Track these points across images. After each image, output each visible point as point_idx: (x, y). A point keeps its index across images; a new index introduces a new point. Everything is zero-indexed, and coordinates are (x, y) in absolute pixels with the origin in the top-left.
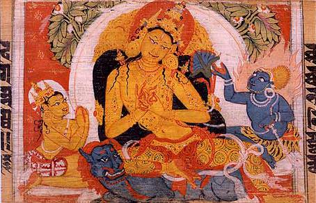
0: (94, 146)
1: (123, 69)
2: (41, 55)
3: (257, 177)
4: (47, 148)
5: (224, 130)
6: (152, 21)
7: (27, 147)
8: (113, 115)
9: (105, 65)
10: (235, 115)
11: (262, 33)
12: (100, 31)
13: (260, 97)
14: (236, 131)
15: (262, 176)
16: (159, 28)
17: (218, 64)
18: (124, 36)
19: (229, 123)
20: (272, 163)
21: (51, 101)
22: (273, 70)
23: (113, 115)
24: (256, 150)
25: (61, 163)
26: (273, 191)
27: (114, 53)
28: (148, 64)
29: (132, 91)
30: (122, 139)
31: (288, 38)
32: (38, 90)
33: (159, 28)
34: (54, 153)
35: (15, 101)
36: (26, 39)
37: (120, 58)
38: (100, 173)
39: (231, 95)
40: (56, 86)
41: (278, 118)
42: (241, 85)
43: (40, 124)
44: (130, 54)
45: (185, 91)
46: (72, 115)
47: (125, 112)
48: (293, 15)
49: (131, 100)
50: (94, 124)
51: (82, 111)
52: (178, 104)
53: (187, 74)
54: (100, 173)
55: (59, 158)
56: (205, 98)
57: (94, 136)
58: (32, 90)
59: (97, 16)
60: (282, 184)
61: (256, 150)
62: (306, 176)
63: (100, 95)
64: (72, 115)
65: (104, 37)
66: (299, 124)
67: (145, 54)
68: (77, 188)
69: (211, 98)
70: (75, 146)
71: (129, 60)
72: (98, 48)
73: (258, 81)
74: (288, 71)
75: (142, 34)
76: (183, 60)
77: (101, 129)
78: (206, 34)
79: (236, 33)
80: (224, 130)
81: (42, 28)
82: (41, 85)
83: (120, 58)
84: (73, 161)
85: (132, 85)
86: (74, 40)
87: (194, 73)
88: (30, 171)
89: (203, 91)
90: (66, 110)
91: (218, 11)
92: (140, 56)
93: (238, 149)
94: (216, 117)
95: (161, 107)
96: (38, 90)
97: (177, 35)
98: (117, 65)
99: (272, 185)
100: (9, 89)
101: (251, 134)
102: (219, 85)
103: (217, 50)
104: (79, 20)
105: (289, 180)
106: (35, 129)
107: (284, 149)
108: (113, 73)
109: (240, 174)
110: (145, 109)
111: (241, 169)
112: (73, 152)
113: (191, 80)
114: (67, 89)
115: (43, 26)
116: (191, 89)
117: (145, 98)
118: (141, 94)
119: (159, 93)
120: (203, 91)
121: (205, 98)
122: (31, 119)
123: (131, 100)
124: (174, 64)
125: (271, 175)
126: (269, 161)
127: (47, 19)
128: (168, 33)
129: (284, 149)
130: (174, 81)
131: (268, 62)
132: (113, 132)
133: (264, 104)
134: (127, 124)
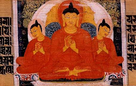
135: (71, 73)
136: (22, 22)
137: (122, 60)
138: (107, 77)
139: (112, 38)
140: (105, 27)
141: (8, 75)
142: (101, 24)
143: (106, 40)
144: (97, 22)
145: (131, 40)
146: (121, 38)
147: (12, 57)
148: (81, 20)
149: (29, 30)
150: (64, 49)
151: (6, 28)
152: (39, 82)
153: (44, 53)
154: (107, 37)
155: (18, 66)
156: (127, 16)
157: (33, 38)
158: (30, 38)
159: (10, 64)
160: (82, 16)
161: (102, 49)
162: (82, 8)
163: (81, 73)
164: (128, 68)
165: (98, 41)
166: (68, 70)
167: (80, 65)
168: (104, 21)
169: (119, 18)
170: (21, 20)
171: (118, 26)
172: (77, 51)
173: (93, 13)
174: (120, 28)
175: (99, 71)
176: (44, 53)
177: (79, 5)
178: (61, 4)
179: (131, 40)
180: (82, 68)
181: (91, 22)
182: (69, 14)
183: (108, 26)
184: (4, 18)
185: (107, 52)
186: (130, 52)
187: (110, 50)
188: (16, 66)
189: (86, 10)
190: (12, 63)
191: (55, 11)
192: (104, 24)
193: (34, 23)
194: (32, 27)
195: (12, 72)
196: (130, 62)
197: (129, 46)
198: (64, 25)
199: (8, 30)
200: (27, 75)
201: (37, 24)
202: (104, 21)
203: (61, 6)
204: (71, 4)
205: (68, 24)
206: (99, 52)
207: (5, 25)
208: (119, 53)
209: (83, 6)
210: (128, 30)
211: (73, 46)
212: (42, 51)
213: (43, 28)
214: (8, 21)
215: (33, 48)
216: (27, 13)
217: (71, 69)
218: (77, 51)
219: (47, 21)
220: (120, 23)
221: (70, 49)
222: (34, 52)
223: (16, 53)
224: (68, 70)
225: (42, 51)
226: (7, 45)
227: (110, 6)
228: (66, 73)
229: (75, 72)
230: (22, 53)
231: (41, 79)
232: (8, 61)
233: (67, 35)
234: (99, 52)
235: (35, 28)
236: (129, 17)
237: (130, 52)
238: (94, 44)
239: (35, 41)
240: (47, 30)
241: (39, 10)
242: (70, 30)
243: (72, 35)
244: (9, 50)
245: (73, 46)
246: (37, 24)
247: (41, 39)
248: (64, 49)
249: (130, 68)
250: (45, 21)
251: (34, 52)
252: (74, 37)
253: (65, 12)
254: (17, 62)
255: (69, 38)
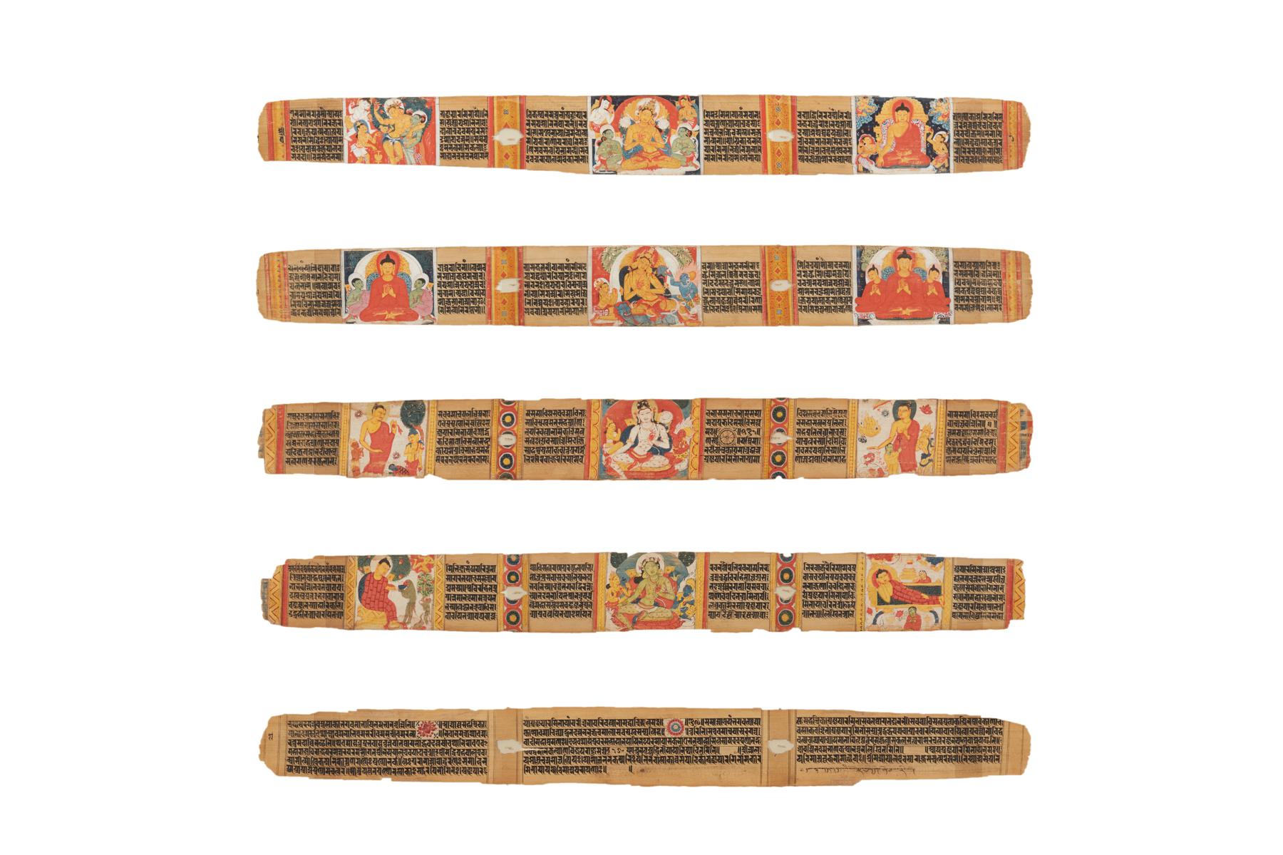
0: (620, 303)
1: (631, 273)
2: (599, 268)
3: (684, 315)
4: (601, 305)
5: (670, 296)
6: (642, 255)
7: (593, 304)
8: (627, 291)
9: (624, 272)
10: (675, 290)
11: (686, 259)
12: (621, 259)
13: (685, 284)
14: (675, 297)
15: (686, 314)
16: (645, 257)
17: (668, 271)
18: (631, 260)
19: (672, 293)
20: (689, 309)
21: (603, 286)
22: (690, 273)
23: (627, 291)
24: (684, 304)
25: (607, 310)
26: (690, 320)
27: (627, 267)
28: (640, 271)
29: (634, 282)
30: (630, 301)
31: (695, 261)
32: (597, 282)
33: (645, 257)
34: (604, 307)
35: (588, 286)
36: (593, 262)
37: (629, 269)
38: (622, 314)
39: (673, 283)
40: (605, 280)
41: (692, 292)
42: (677, 279)
43: (598, 295)
44: (634, 267)
45: (655, 281)
46: (611, 292)
47: (632, 290)
48: (697, 252)
49: (634, 285)
50: (620, 295)
51: (615, 290)
52: (652, 287)
53: (656, 275)
54: (622, 314)
55: (606, 308)
56: (663, 284)
57: (620, 300)
58: (595, 282)
59: (620, 253)
60: (694, 317)
61: (684, 304)
62: (703, 314)
63: (622, 283)
64: (611, 292)
65: (623, 260)
66: (700, 294)
67: (639, 267)
68: (613, 320)
69: (665, 284)
70: (612, 304)
71: (633, 270)
72: (620, 266)
73: (684, 277)
74: (695, 273)
75: (638, 259)
76: (654, 269)
77: (623, 297)
78: (663, 259)
79: (675, 258)
80: (670, 296)
81: (599, 258)
82: (599, 280)
83: (629, 269)
84: (611, 310)
85: (634, 279)
86: (612, 261)
87: (659, 274)
88: (595, 314)
89: (662, 281)
90: (608, 290)
91: (668, 250)
92: (637, 268)
93: (676, 304)
94: (667, 291)
95: (646, 288)
96: (597, 282)
97: (652, 259)
98: (628, 272)
99: (690, 318)
100: (586, 282)
101: (681, 298)
102: (668, 279)
103: (667, 266)
104: (613, 254)
105: (696, 316)
106: (597, 297)
107: (694, 303)
108: (627, 275)
109: (677, 313)
110: (639, 289)
111: (677, 312)
112: (611, 306)
113: (658, 277)
114: (609, 281)
115: (599, 257)
116: (657, 281)
117: (639, 285)
118: (638, 283)
119: (645, 282)
120: (662, 281)
121: (663, 284)
122: (595, 294)
123: (634, 285)
124: (651, 271)
125: (689, 314)
126: (687, 309)
127: (600, 255)
128: (648, 259)
129: (694, 303)
130: (651, 278)
131: (687, 270)
132: (627, 298)
133: (686, 286)
134: (632, 295)
135: (904, 312)
136: (861, 265)
137: (950, 301)
138: (936, 316)
139: (941, 281)
140: (935, 271)
141: (847, 313)
142: (931, 269)
143: (936, 283)
144: (928, 266)
145: (958, 283)
146: (948, 281)
147: (851, 298)
148: (913, 265)
149: (866, 273)
150: (898, 291)
151: (846, 271)
152: (875, 319)
153: (880, 294)
154: (937, 280)
155: (856, 305)
156: (955, 262)
157: (871, 281)
158: (867, 281)
159: (849, 304)
160: (914, 261)
161: (932, 291)
162: (914, 254)
163: (913, 313)
164: (955, 308)
165: (928, 284)
166: (901, 309)
167: (912, 306)
168: (934, 266)
169: (948, 264)
170: (860, 264)
171: (946, 271)
172: (909, 292)
173: (924, 259)
174: (948, 273)
175: (929, 310)
176: (880, 294)
177: (912, 251)
178: (896, 251)
179: (958, 283)
180: (914, 307)
181: (923, 267)
182: (902, 260)
183: (938, 271)
184: (845, 262)
185: (936, 293)
186: (956, 294)
187: (938, 292)
188: (854, 305)
189: (918, 256)
190: (851, 303)
191: (890, 257)
192: (933, 268)
193: (871, 267)
194: (870, 270)
195: (851, 311)
196: (956, 303)
197: (956, 288)
198: (898, 269)
199: (848, 273)
200: (864, 314)
201: (873, 268)
202: (934, 266)
203: (896, 252)
204: (905, 250)
205: (902, 268)
206: (929, 294)
207: (845, 269)
208: (947, 295)
209: (916, 252)
210: (955, 274)
211: (906, 289)
212: (878, 292)
213: (879, 271)
214: (848, 264)
215: (870, 290)
216: (865, 258)
217: (904, 308)
218: (909, 292)
219: (883, 266)
220: (948, 268)
221: (903, 291)
222: (871, 293)
223: (855, 294)
224: (901, 309)
225: (878, 292)
226: (847, 287)
227: (939, 253)
228: (899, 312)
229: (908, 312)
230: (860, 294)
231: (877, 318)
232: (848, 301)
233: (901, 278)
234: (929, 294)
235: (872, 271)
236: (956, 263)
237: (956, 294)
238: (925, 286)
239: (872, 283)
240: (883, 274)
241: (876, 255)
242: (904, 274)
243: (905, 278)
244: (849, 291)
245: (906, 289)
246: (873, 268)
247: (877, 281)
248: (898, 291)
249: (956, 308)
250: (881, 265)
251: (871, 293)
252: (907, 280)
253: (899, 258)
254: (856, 302)
255: (902, 281)
